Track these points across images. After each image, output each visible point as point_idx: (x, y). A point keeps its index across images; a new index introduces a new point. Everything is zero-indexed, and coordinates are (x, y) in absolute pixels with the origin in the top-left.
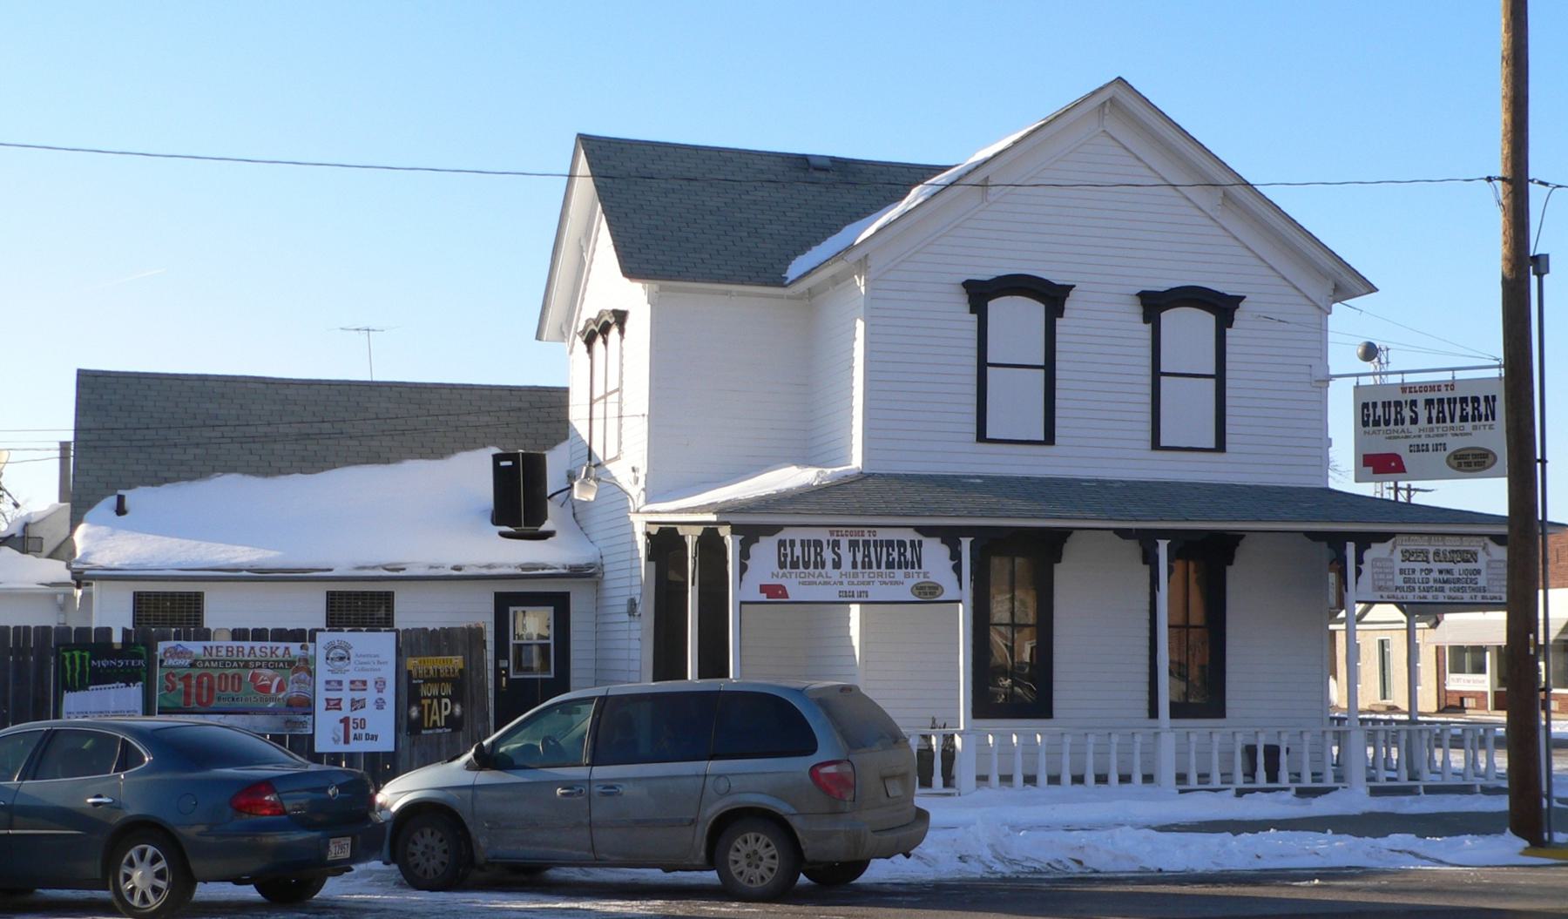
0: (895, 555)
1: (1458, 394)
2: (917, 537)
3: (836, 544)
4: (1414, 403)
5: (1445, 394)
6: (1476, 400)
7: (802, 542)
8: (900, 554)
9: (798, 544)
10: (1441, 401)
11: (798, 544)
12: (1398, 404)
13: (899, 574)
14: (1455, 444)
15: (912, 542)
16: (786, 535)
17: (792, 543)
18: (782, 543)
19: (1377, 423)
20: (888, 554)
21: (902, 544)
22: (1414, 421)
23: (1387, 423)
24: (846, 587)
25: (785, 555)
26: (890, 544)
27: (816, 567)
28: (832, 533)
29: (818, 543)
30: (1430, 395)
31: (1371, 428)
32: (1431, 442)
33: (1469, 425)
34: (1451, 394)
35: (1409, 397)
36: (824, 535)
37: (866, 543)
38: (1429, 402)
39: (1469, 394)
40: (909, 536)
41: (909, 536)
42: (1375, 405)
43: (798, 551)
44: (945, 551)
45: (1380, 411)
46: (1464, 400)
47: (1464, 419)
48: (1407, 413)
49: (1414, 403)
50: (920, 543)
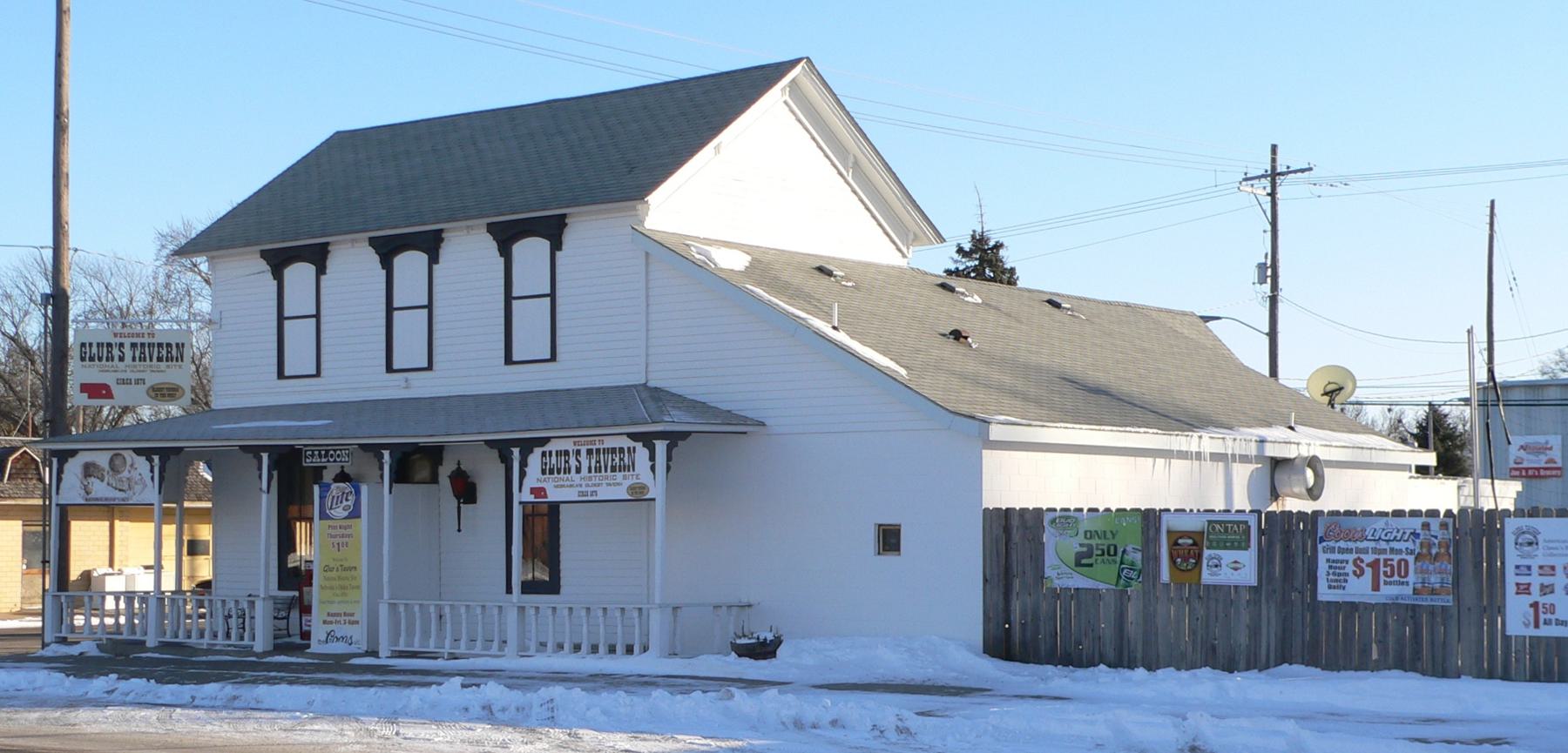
1: (155, 341)
2: (631, 444)
3: (578, 452)
4: (122, 345)
5: (146, 340)
6: (169, 345)
10: (143, 345)
12: (109, 345)
16: (547, 448)
18: (544, 454)
21: (622, 450)
22: (121, 359)
23: (100, 359)
29: (567, 453)
30: (135, 340)
31: (87, 363)
34: (151, 340)
35: (118, 340)
38: (133, 345)
39: (164, 341)
41: (626, 443)
44: (646, 452)
46: (160, 345)
48: (116, 352)
49: (122, 345)
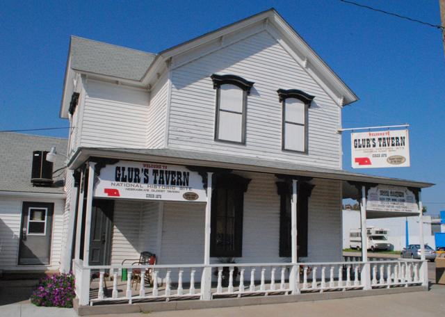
0: (176, 178)
2: (187, 171)
3: (146, 171)
4: (374, 139)
6: (397, 138)
7: (129, 169)
8: (178, 178)
9: (126, 169)
10: (384, 139)
11: (126, 169)
12: (368, 140)
13: (177, 188)
14: (389, 154)
15: (184, 173)
16: (120, 165)
17: (124, 169)
18: (118, 169)
19: (360, 147)
20: (172, 178)
21: (179, 173)
22: (374, 146)
23: (364, 146)
24: (150, 193)
25: (119, 175)
26: (173, 173)
27: (135, 182)
28: (145, 166)
29: (137, 170)
31: (358, 148)
32: (381, 153)
33: (395, 147)
35: (372, 137)
36: (140, 167)
37: (162, 172)
38: (380, 139)
40: (182, 170)
42: (359, 140)
43: (126, 173)
44: (200, 178)
45: (361, 142)
46: (393, 138)
47: (393, 145)
48: (371, 143)
49: (374, 139)
50: (188, 174)
